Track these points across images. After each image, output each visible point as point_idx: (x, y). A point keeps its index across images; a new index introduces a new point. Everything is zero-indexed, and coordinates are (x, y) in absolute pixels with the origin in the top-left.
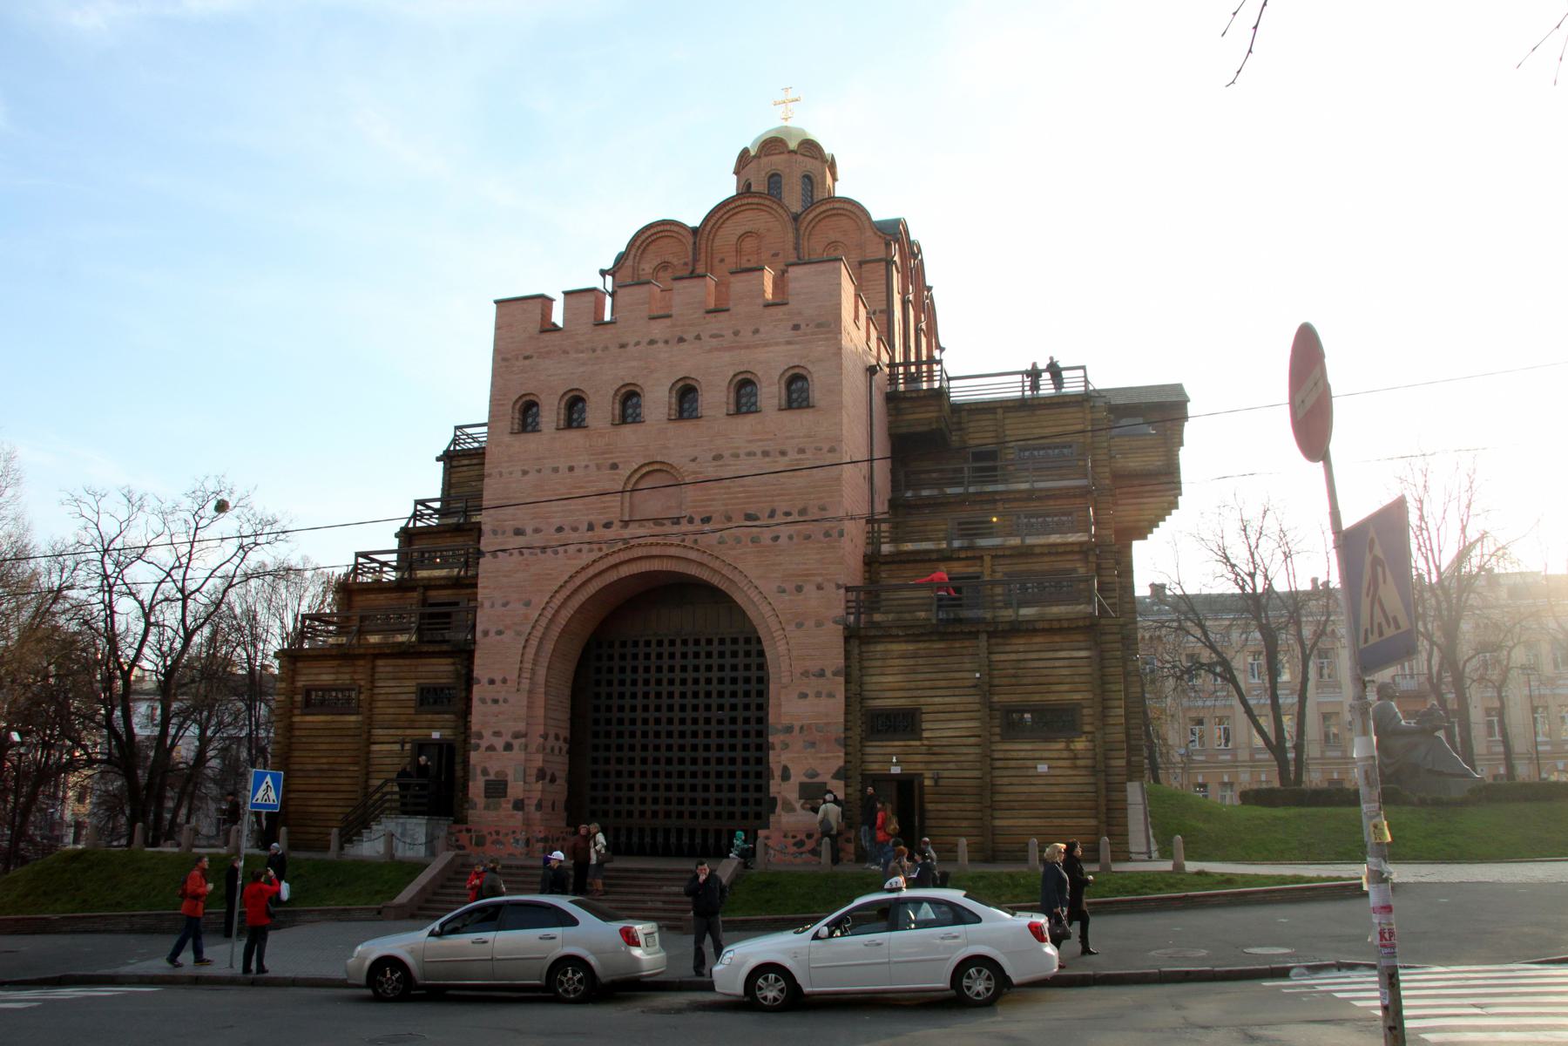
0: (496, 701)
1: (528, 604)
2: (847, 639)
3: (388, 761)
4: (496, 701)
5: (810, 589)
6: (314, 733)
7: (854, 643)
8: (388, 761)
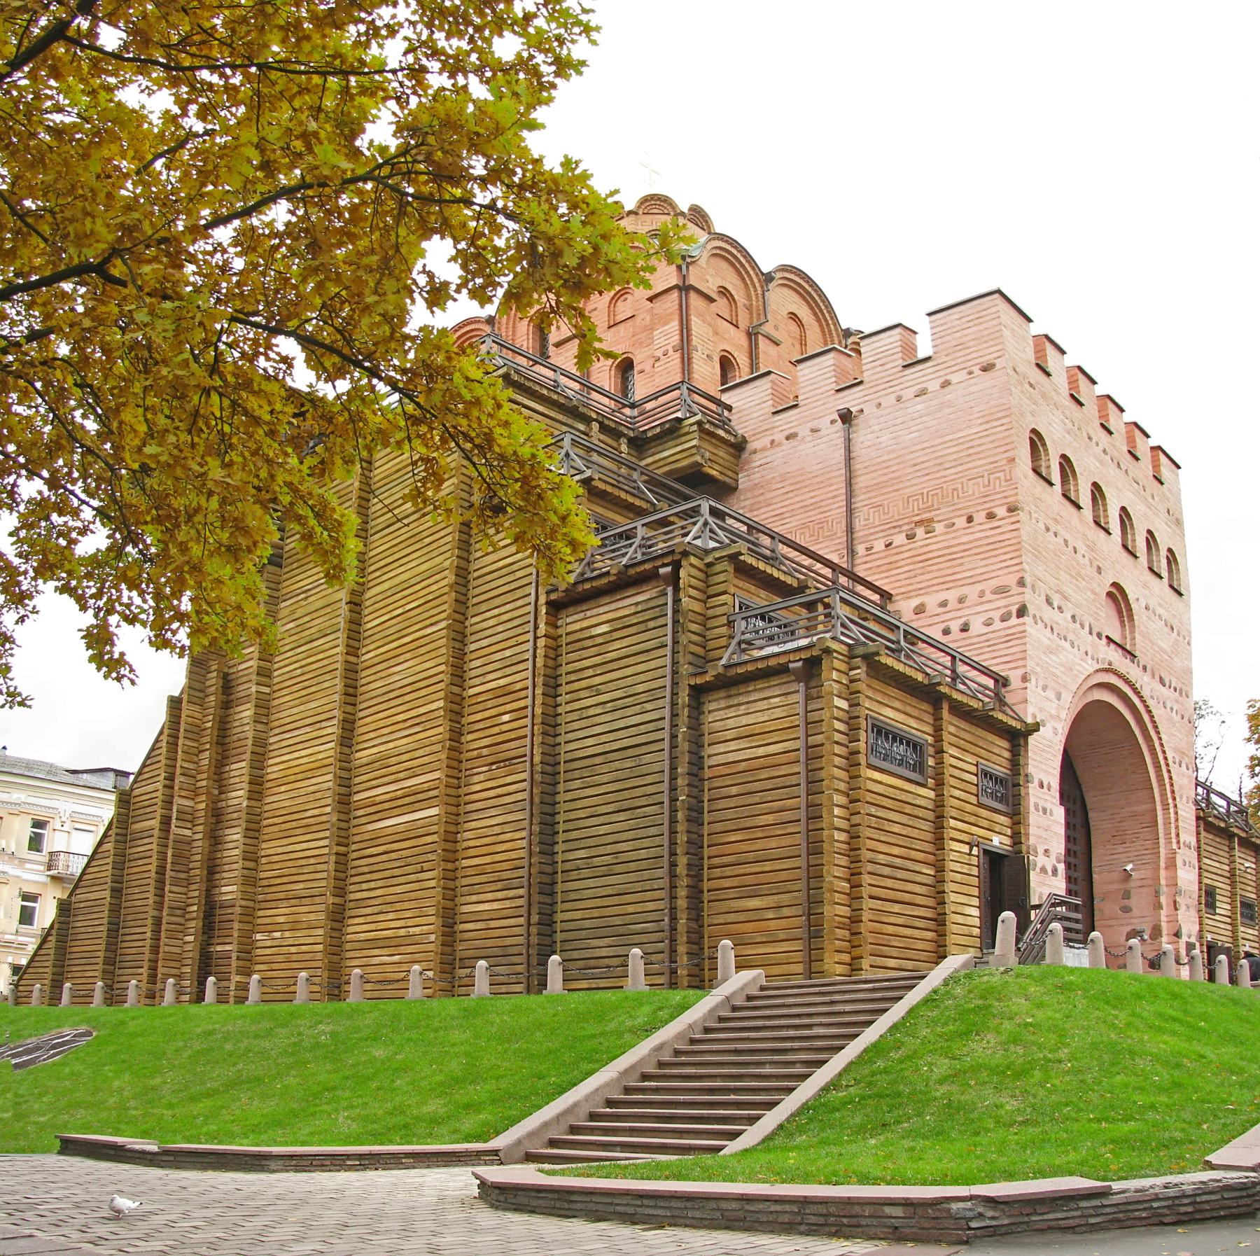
0: (1045, 813)
1: (1059, 697)
2: (1198, 818)
3: (957, 867)
4: (1045, 811)
5: (1184, 765)
6: (886, 802)
7: (1201, 823)
8: (957, 867)
